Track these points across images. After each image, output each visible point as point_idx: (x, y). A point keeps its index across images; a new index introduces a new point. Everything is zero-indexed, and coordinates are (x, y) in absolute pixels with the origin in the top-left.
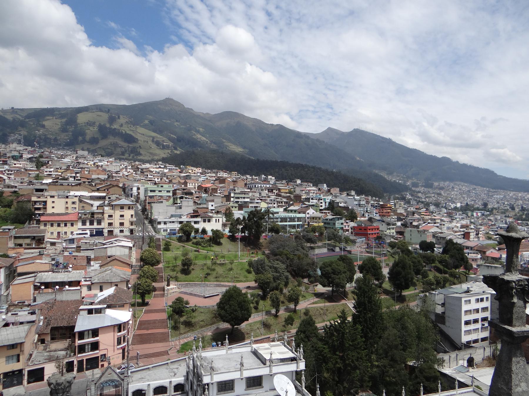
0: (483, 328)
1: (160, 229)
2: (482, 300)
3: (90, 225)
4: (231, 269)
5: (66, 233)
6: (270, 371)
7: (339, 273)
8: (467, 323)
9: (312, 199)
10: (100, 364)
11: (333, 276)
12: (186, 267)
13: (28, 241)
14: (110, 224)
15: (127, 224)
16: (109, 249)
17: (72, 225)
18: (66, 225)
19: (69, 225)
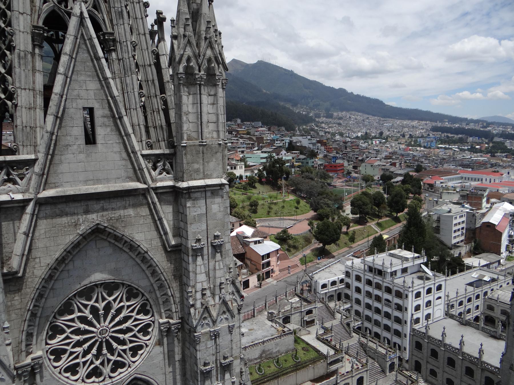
0: (462, 234)
2: (462, 216)
4: (283, 207)
8: (455, 231)
9: (277, 141)
11: (363, 207)
12: (254, 208)
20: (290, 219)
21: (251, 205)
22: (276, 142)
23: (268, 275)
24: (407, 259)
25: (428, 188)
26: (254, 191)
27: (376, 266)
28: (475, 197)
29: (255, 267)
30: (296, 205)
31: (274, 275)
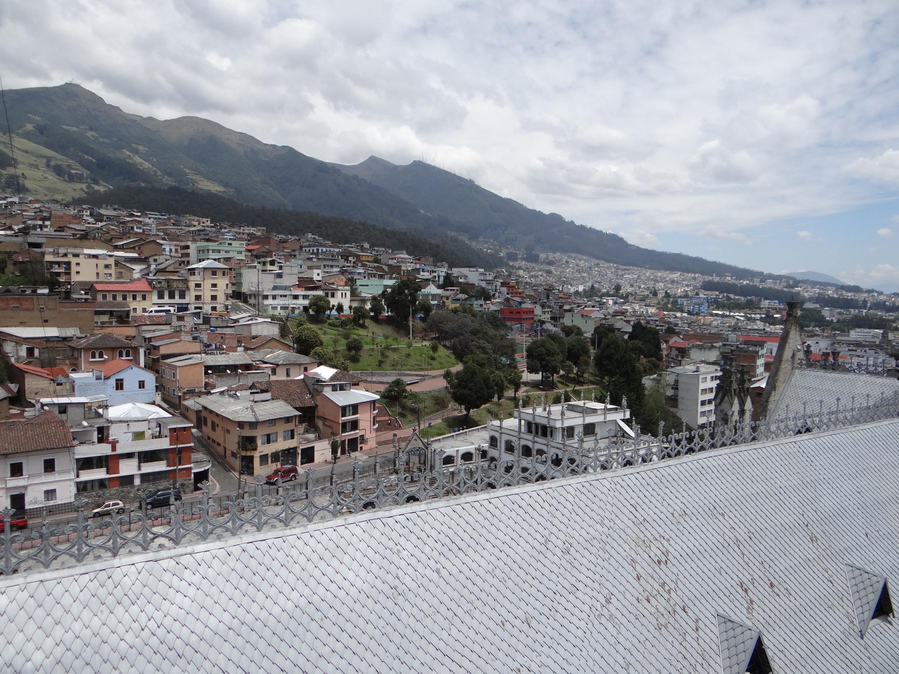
1: (267, 305)
3: (180, 298)
4: (408, 355)
5: (135, 310)
6: (605, 418)
7: (553, 355)
8: (703, 403)
9: (423, 271)
10: (359, 446)
12: (353, 352)
13: (105, 318)
14: (198, 298)
15: (221, 298)
16: (253, 327)
17: (144, 298)
18: (134, 298)
19: (139, 298)
20: (417, 375)
21: (350, 348)
22: (422, 273)
23: (354, 445)
24: (594, 411)
25: (677, 356)
26: (362, 332)
27: (538, 420)
28: (745, 356)
29: (330, 431)
30: (431, 353)
31: (365, 447)
